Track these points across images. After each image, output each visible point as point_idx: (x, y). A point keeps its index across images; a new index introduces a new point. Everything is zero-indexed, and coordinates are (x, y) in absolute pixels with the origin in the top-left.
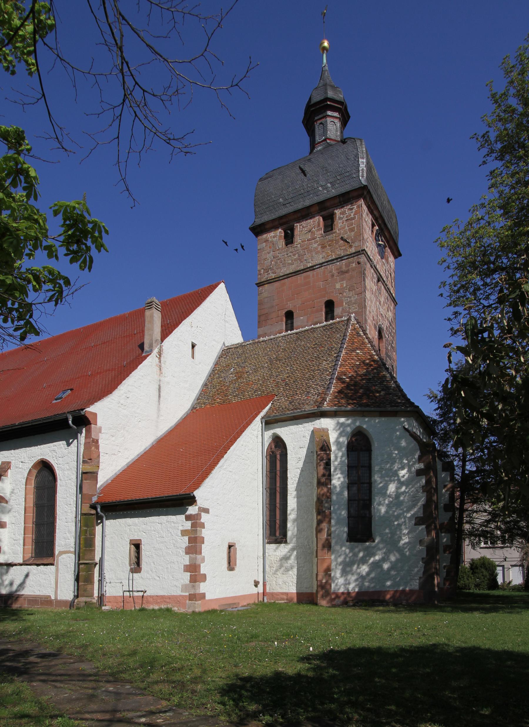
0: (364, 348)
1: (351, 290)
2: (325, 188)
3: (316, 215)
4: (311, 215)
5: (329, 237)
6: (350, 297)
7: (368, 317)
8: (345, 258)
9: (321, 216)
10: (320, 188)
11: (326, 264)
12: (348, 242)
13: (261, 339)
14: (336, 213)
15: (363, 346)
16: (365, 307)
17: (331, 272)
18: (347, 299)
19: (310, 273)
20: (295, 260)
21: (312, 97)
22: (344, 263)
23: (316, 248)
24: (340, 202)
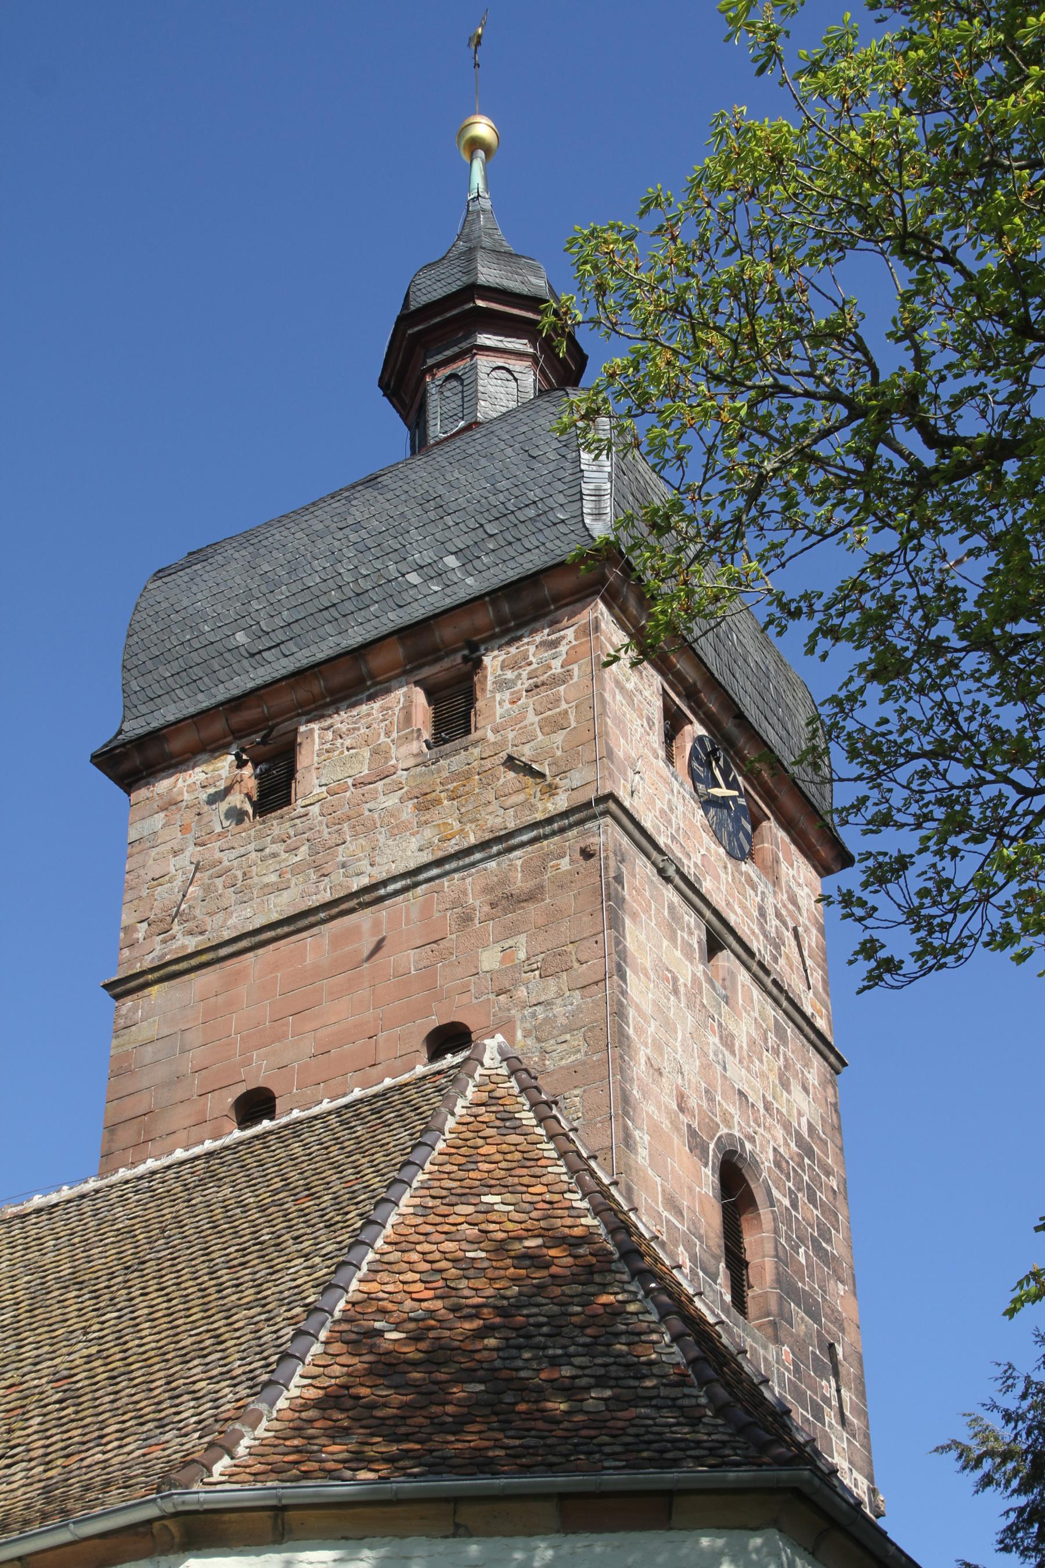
0: (526, 1180)
1: (550, 971)
3: (394, 683)
4: (375, 684)
5: (456, 763)
6: (548, 1004)
7: (645, 1094)
8: (525, 838)
9: (417, 683)
11: (435, 872)
12: (542, 775)
15: (525, 1171)
16: (622, 1039)
17: (456, 903)
18: (534, 1015)
21: (413, 289)
22: (519, 862)
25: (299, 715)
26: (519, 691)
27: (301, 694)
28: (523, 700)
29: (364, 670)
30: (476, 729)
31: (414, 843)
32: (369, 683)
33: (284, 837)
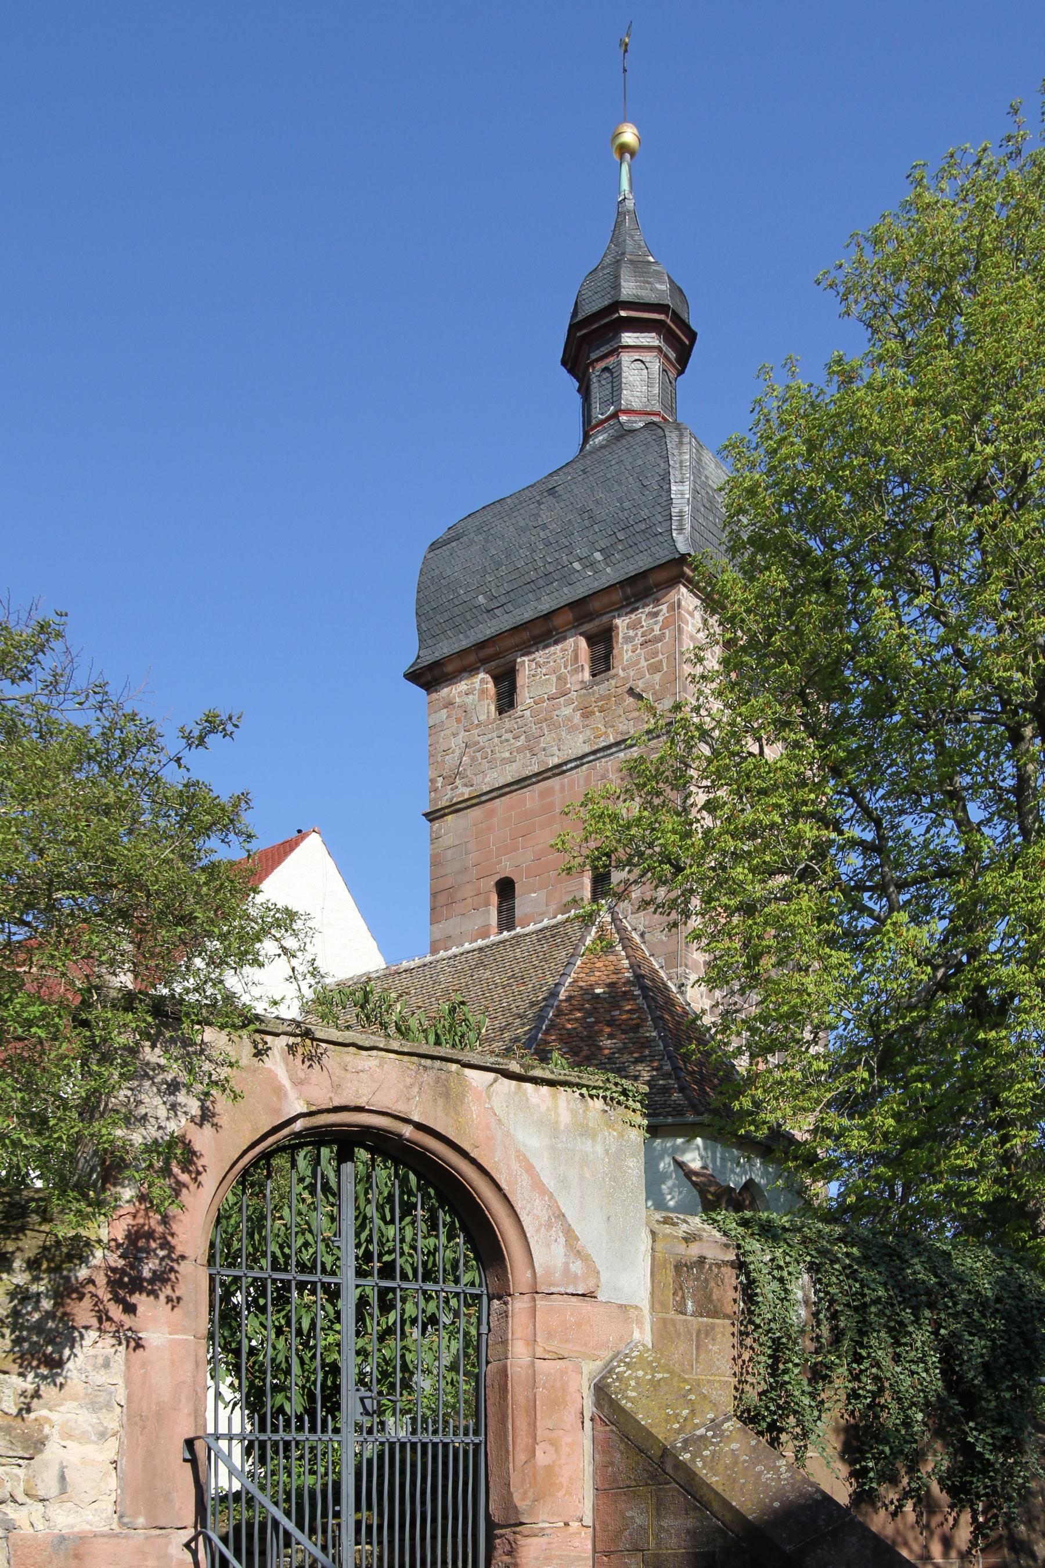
2: (588, 563)
5: (601, 689)
10: (577, 566)
13: (442, 954)
14: (617, 627)
19: (555, 783)
20: (519, 750)
23: (569, 719)
24: (627, 598)
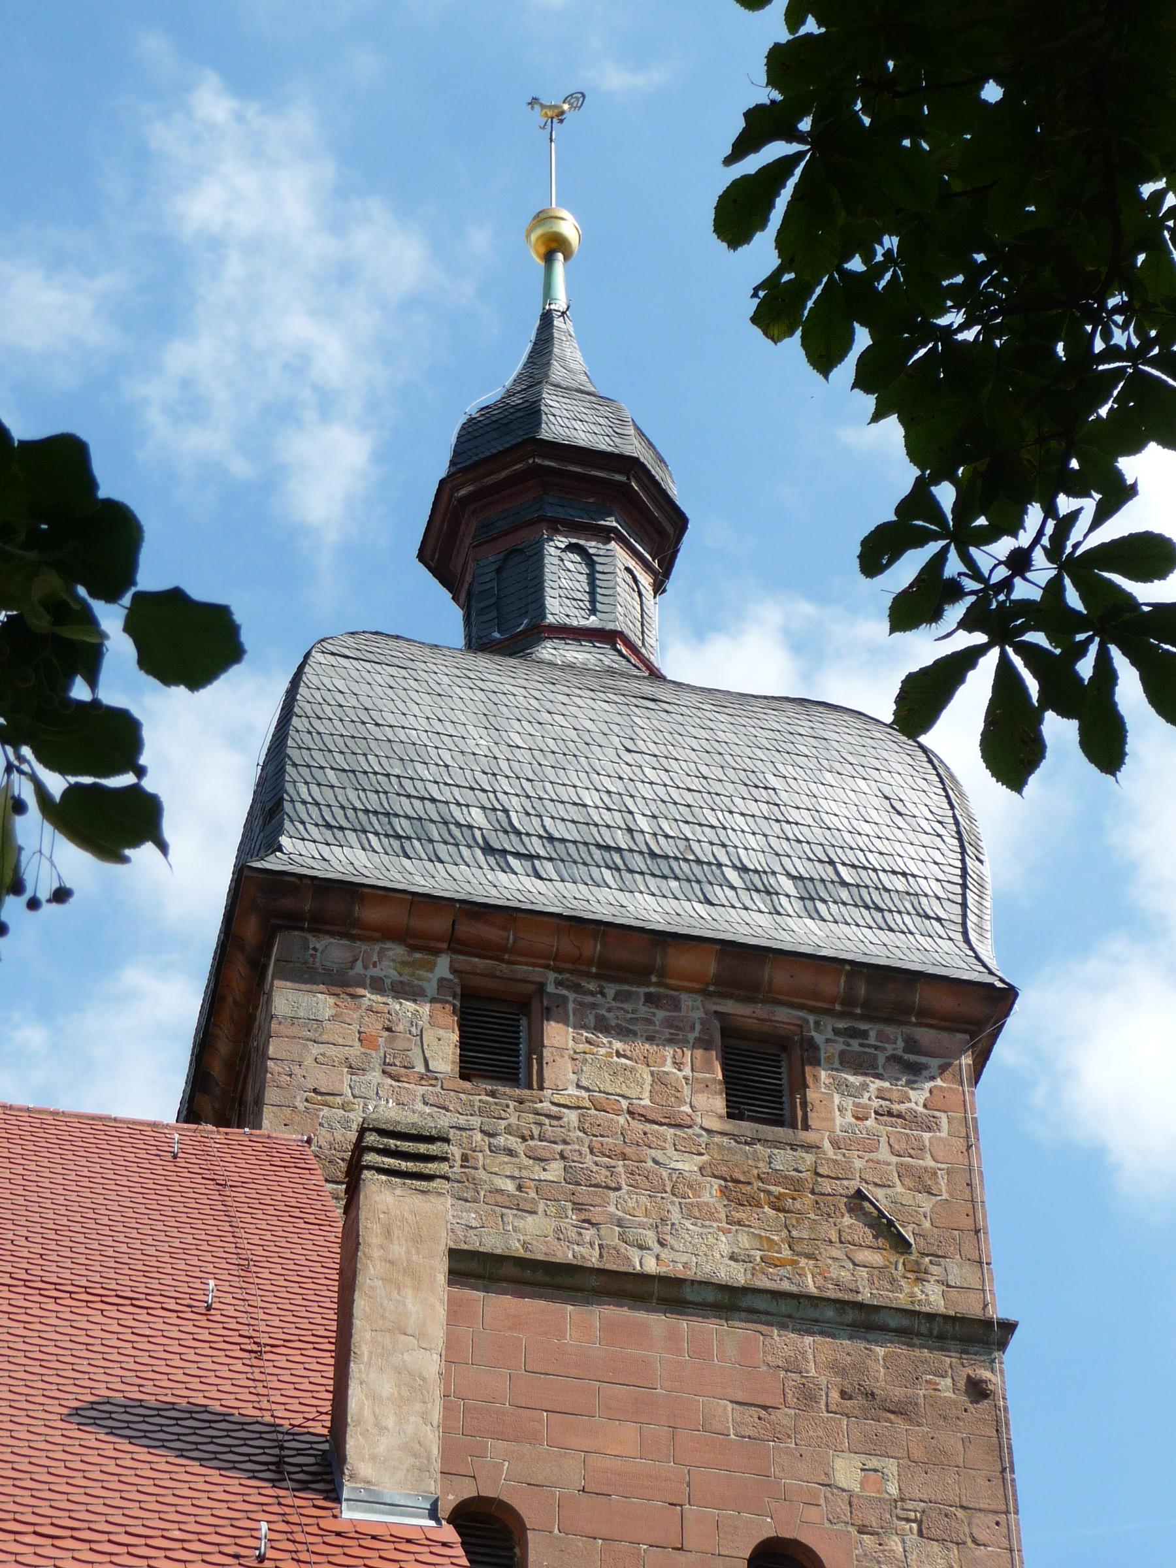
25: (547, 967)
26: (865, 1107)
27: (567, 945)
28: (870, 1123)
29: (658, 960)
30: (806, 1127)
31: (724, 1245)
32: (654, 979)
33: (527, 1133)
